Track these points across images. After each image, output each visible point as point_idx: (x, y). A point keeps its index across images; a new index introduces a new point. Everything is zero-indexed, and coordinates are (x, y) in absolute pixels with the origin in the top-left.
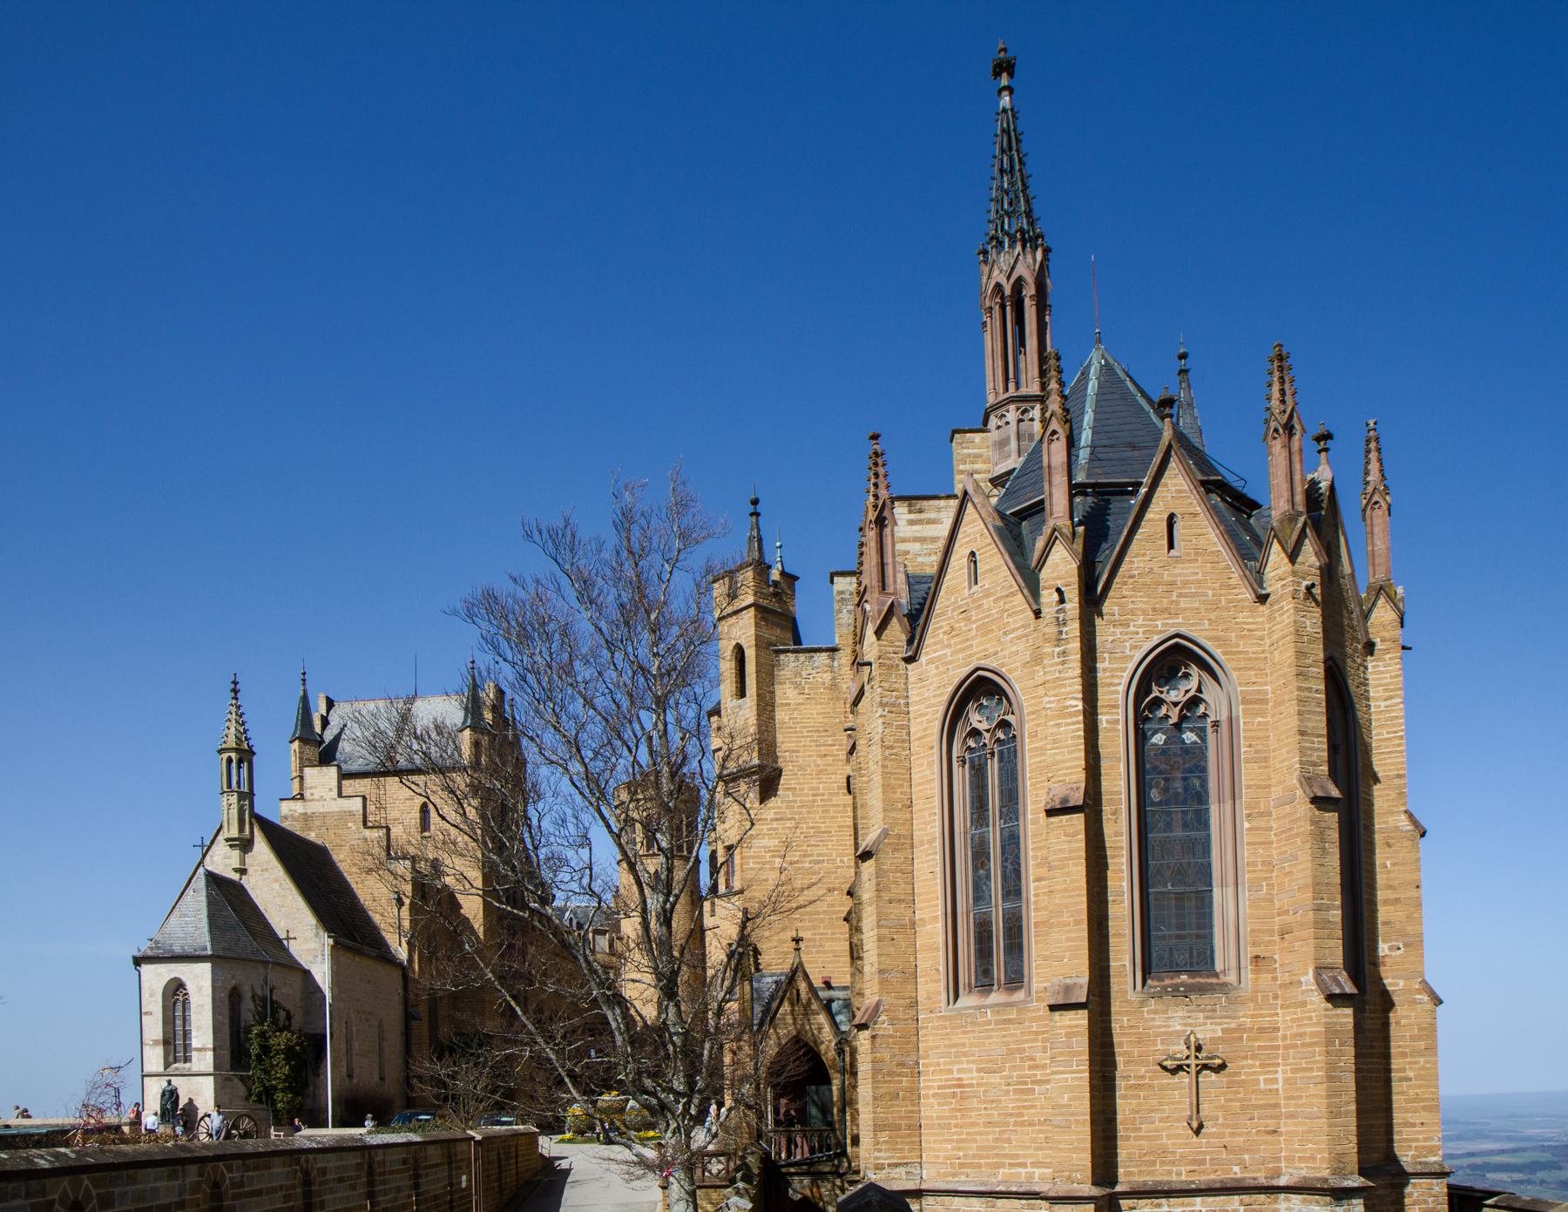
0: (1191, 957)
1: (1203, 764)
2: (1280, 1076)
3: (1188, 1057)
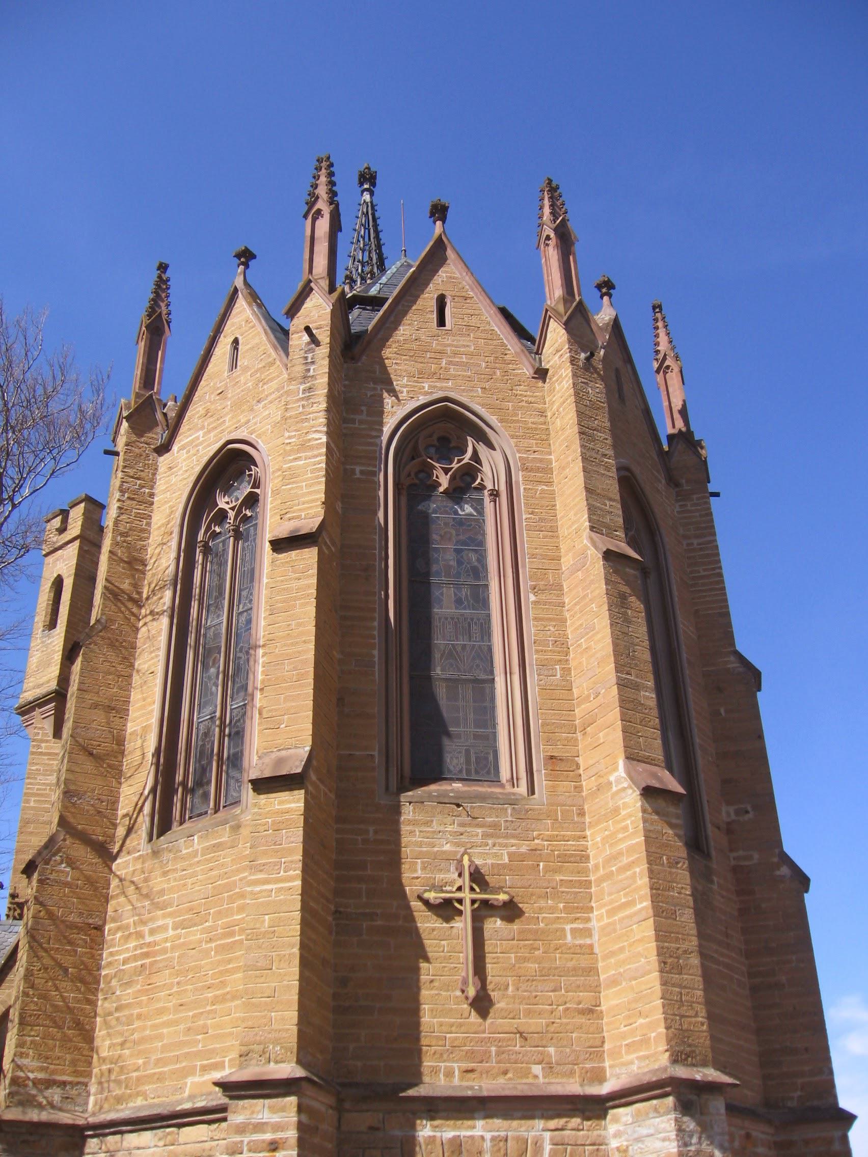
0: (468, 762)
1: (480, 537)
2: (595, 924)
3: (460, 889)
